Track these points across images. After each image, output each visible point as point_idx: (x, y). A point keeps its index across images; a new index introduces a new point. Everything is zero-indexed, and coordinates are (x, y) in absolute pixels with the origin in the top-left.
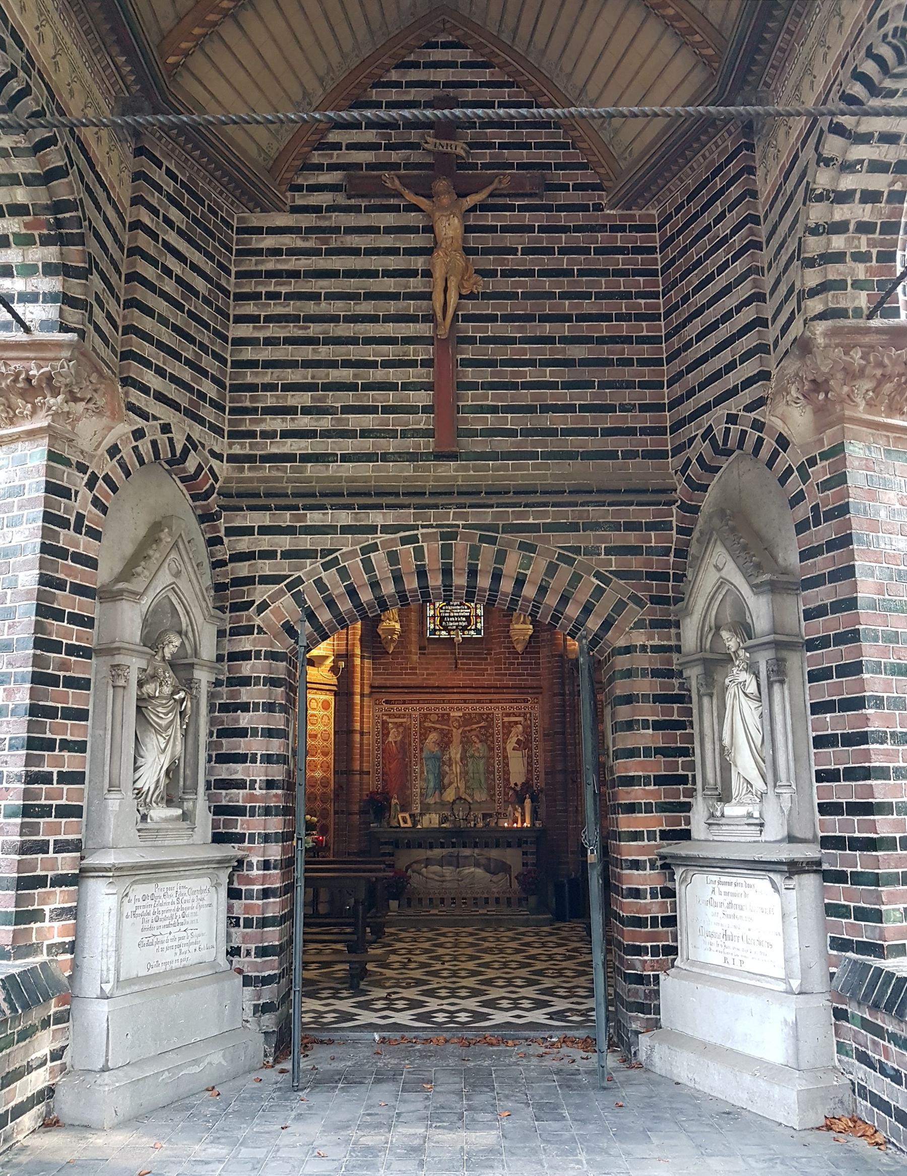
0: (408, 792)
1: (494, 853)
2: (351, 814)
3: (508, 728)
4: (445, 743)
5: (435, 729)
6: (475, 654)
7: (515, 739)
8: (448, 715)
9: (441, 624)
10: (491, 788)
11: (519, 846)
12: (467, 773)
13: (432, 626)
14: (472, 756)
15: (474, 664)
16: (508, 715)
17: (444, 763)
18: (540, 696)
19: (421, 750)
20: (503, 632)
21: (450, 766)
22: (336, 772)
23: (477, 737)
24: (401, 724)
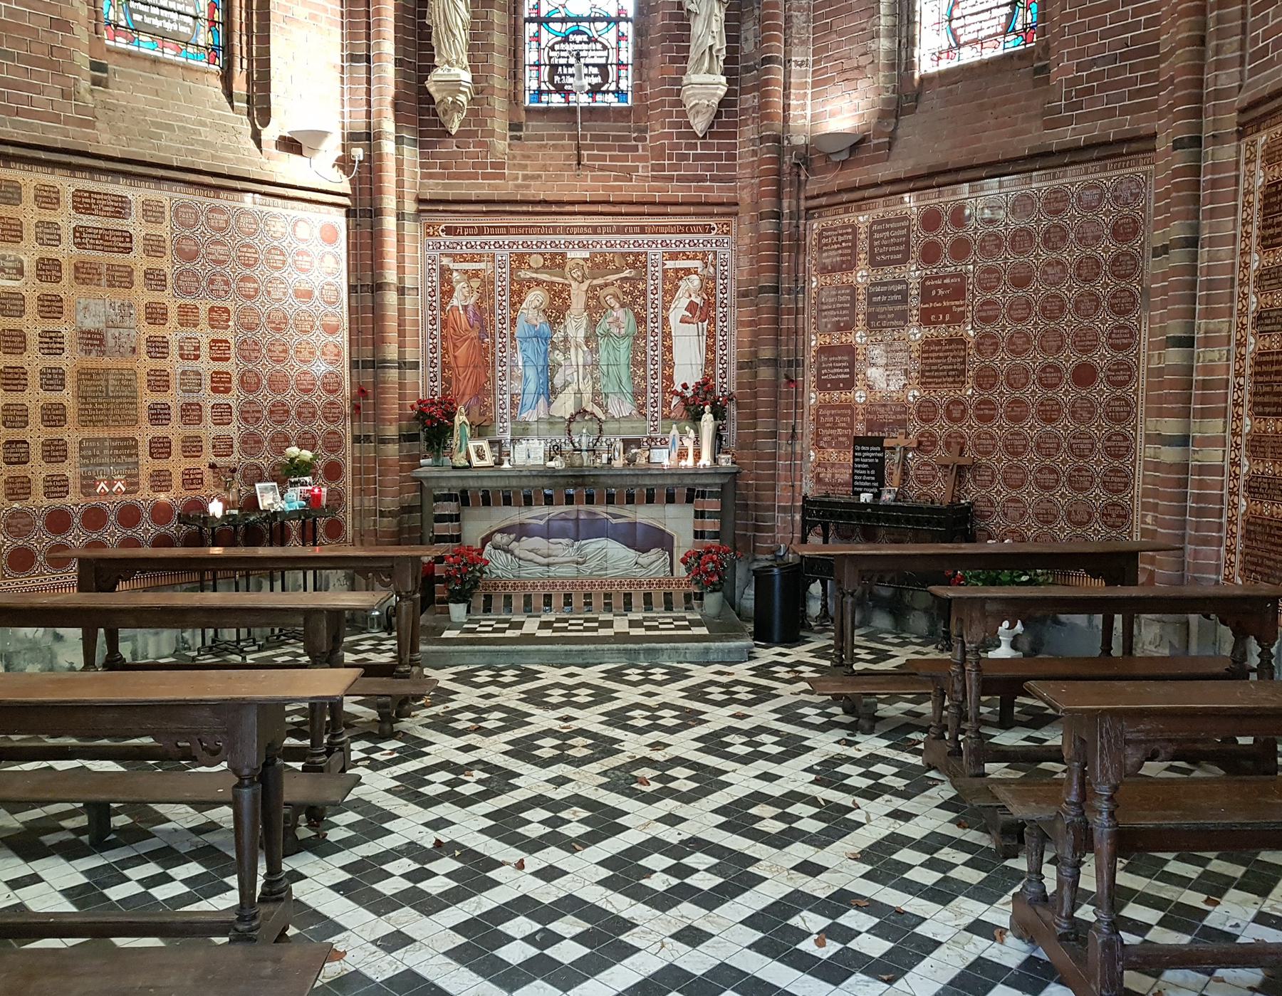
0: (488, 401)
1: (644, 515)
2: (383, 441)
4: (556, 311)
5: (539, 283)
6: (616, 138)
8: (563, 255)
9: (551, 81)
10: (638, 394)
11: (690, 500)
12: (596, 365)
13: (534, 85)
14: (607, 334)
15: (612, 158)
16: (674, 256)
20: (668, 93)
21: (567, 350)
22: (354, 364)
23: (616, 296)
24: (476, 274)
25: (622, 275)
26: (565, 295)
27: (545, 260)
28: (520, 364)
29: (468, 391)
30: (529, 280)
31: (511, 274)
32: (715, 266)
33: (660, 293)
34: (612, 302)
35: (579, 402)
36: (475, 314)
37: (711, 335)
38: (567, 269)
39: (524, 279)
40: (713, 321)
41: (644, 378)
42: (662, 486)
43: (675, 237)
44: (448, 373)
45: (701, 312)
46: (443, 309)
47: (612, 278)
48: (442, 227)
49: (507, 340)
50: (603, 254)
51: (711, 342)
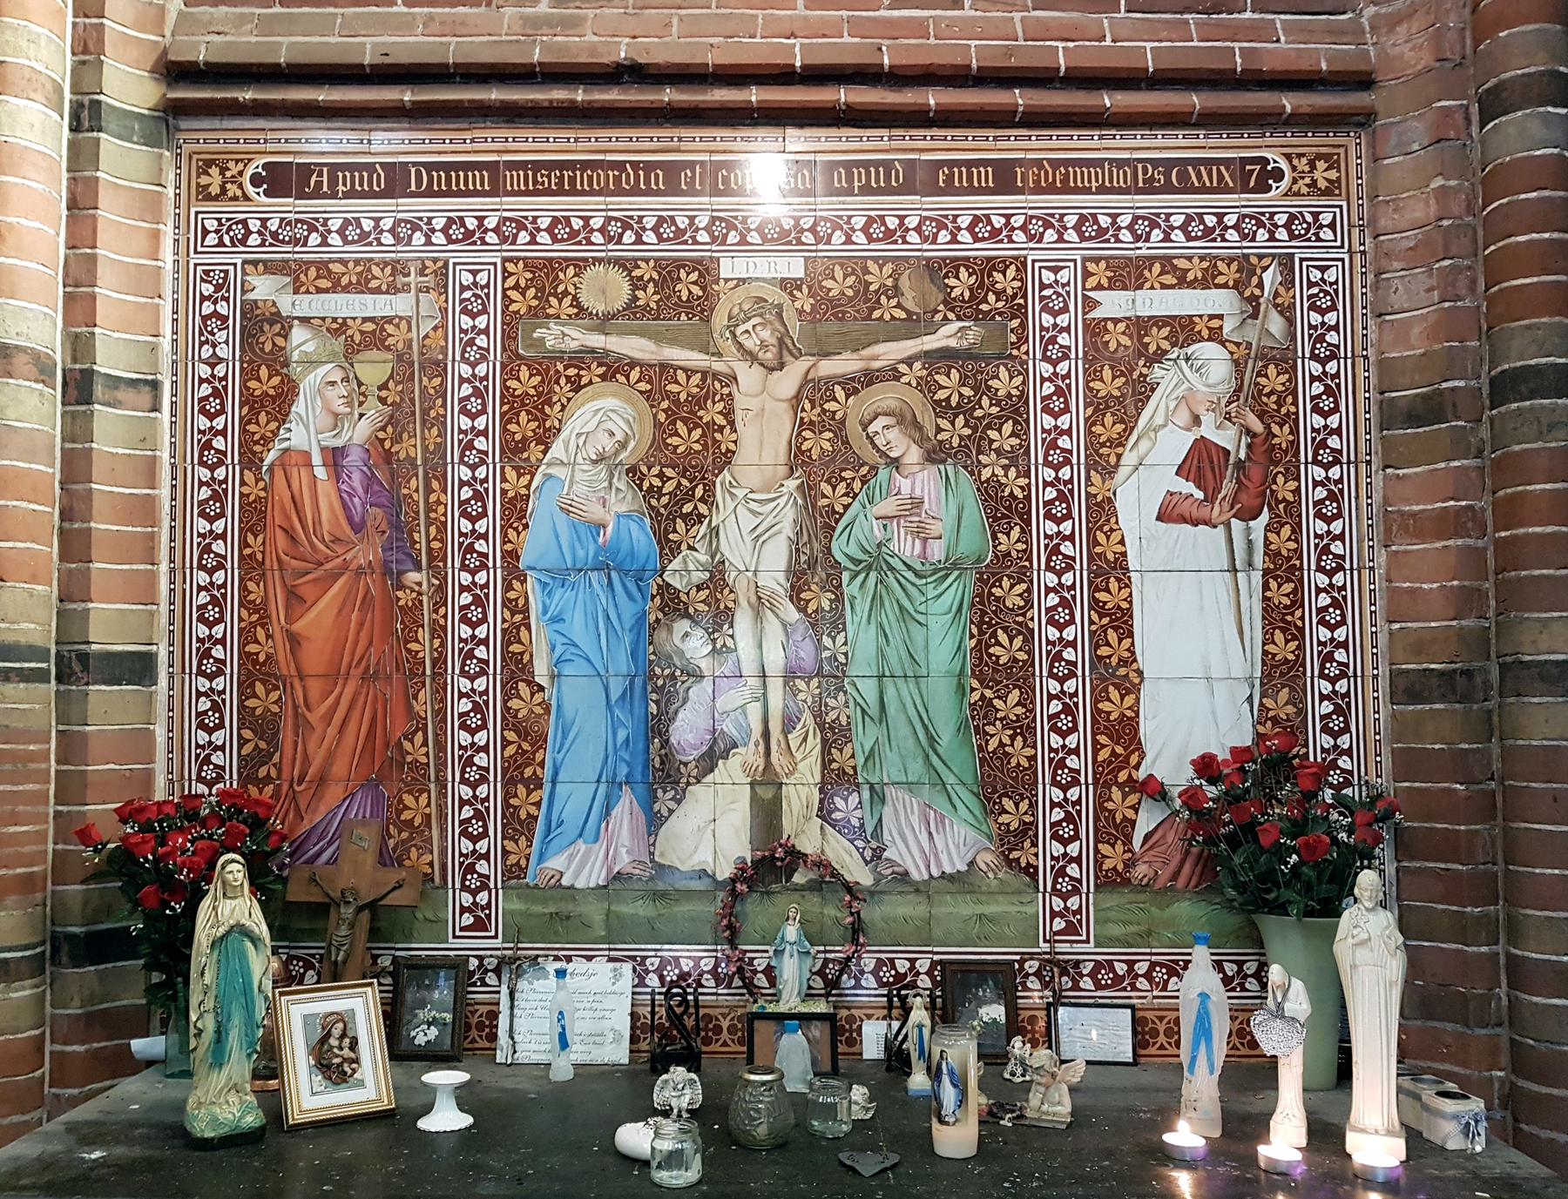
3: (1125, 369)
5: (614, 368)
7: (1175, 444)
8: (705, 270)
10: (1000, 783)
12: (834, 675)
14: (875, 561)
16: (1128, 275)
17: (672, 604)
18: (1353, 146)
19: (516, 511)
21: (722, 617)
23: (907, 421)
24: (376, 335)
25: (931, 342)
26: (712, 413)
27: (637, 284)
29: (339, 768)
30: (580, 358)
31: (509, 337)
32: (1287, 312)
33: (1079, 411)
35: (767, 814)
36: (370, 481)
37: (1282, 568)
38: (719, 320)
39: (558, 356)
40: (1288, 515)
41: (1024, 729)
43: (1129, 205)
44: (264, 700)
45: (1241, 480)
46: (250, 460)
47: (889, 352)
48: (256, 166)
49: (492, 578)
50: (855, 267)
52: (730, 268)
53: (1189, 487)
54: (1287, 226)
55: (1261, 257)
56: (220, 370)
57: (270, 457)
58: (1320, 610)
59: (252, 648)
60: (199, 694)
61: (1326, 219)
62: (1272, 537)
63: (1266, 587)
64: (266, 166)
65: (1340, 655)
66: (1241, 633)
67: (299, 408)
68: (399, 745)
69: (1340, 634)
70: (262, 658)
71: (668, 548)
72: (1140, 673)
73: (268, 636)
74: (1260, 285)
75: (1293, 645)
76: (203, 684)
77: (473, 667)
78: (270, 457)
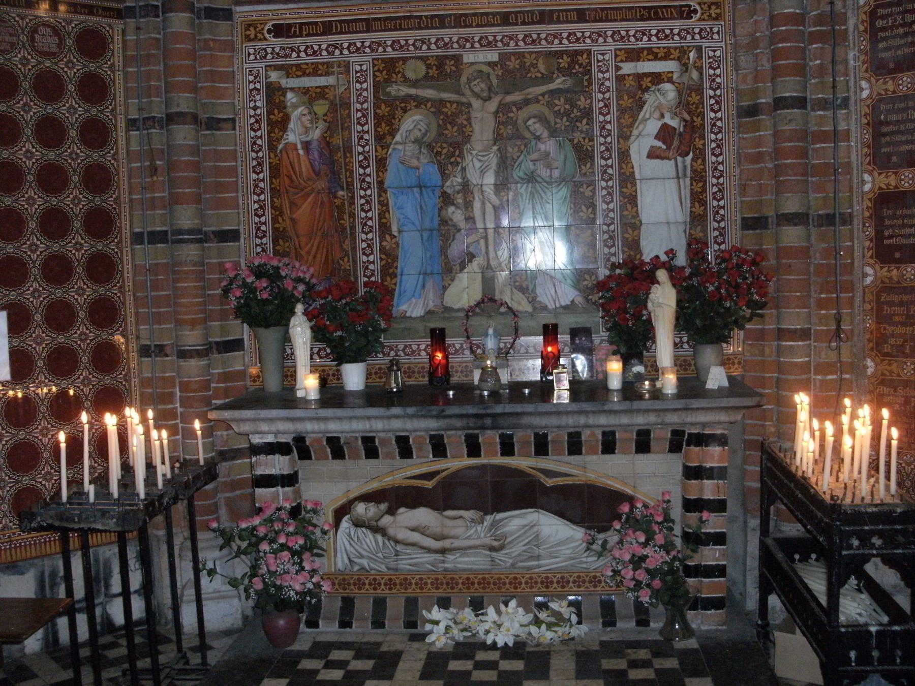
5: (420, 102)
7: (653, 126)
8: (457, 59)
11: (675, 447)
16: (634, 55)
19: (382, 164)
23: (542, 120)
25: (552, 86)
26: (461, 120)
27: (429, 67)
28: (394, 229)
30: (406, 99)
31: (376, 92)
32: (700, 69)
34: (536, 127)
36: (321, 154)
37: (698, 177)
38: (464, 79)
39: (396, 98)
40: (700, 155)
42: (625, 428)
43: (634, 26)
45: (681, 141)
46: (272, 148)
49: (373, 192)
50: (520, 56)
51: (698, 187)
52: (468, 58)
53: (659, 144)
54: (700, 33)
55: (688, 47)
56: (258, 112)
57: (280, 147)
58: (713, 194)
59: (277, 225)
60: (257, 245)
61: (715, 30)
62: (694, 164)
63: (691, 184)
64: (273, 25)
65: (722, 212)
66: (681, 203)
67: (291, 125)
68: (338, 262)
69: (722, 203)
70: (281, 229)
71: (444, 176)
72: (641, 222)
73: (284, 220)
74: (688, 59)
75: (702, 208)
76: (258, 241)
77: (366, 229)
78: (280, 147)
